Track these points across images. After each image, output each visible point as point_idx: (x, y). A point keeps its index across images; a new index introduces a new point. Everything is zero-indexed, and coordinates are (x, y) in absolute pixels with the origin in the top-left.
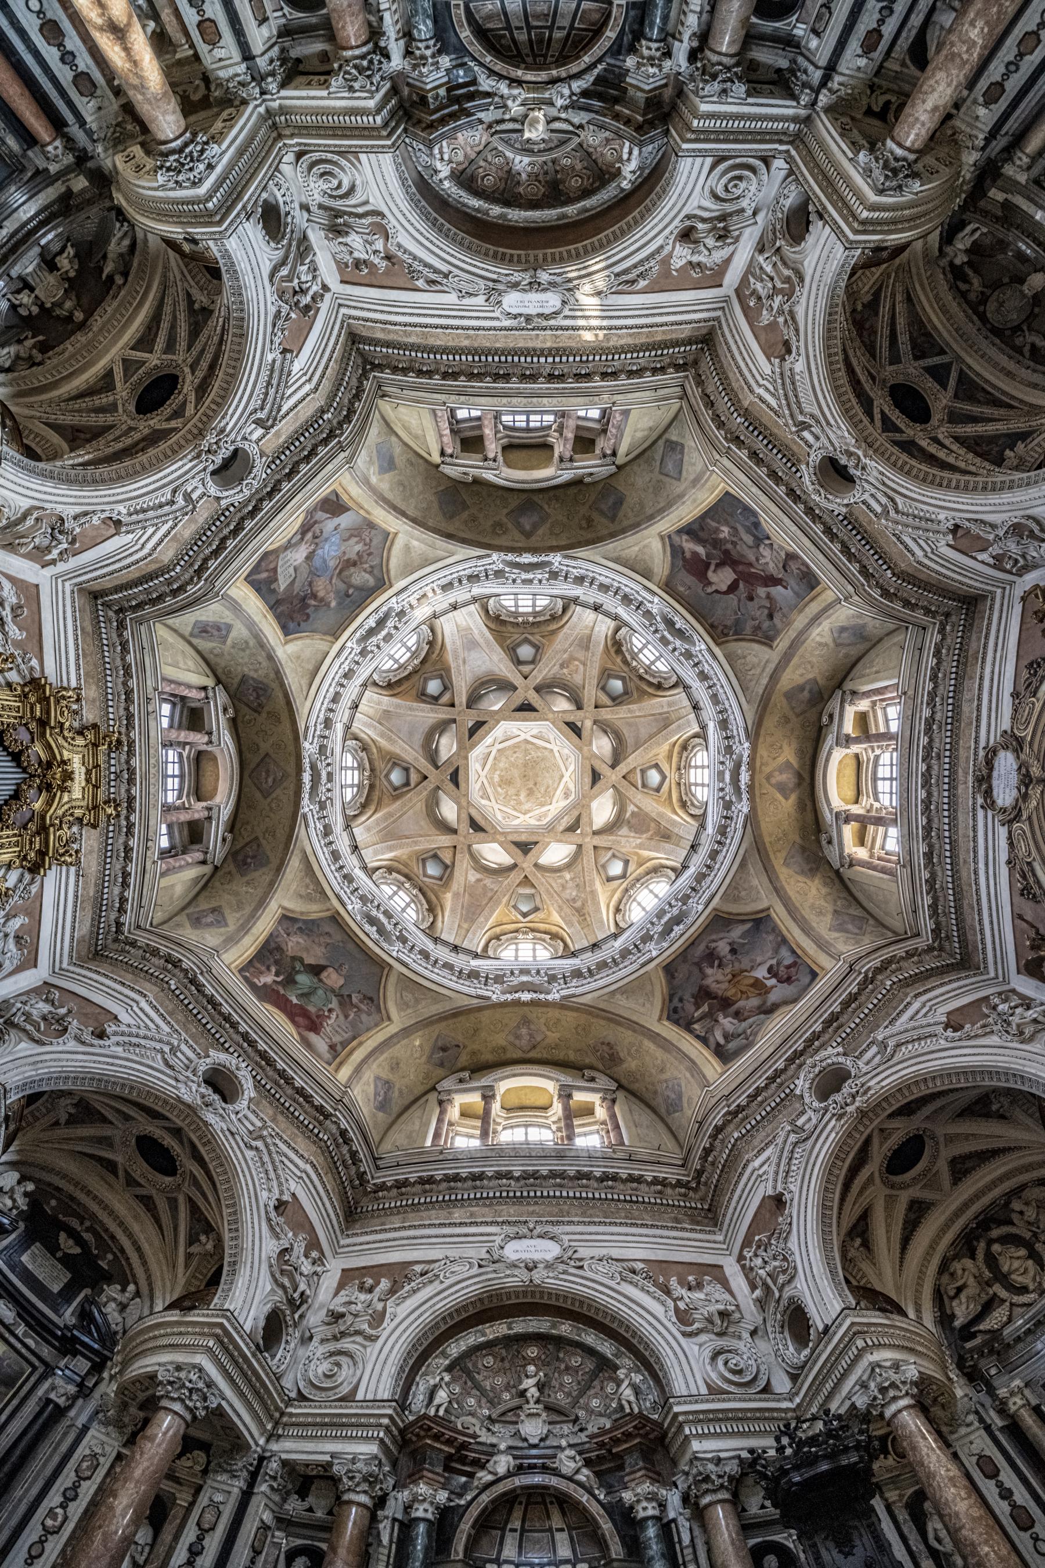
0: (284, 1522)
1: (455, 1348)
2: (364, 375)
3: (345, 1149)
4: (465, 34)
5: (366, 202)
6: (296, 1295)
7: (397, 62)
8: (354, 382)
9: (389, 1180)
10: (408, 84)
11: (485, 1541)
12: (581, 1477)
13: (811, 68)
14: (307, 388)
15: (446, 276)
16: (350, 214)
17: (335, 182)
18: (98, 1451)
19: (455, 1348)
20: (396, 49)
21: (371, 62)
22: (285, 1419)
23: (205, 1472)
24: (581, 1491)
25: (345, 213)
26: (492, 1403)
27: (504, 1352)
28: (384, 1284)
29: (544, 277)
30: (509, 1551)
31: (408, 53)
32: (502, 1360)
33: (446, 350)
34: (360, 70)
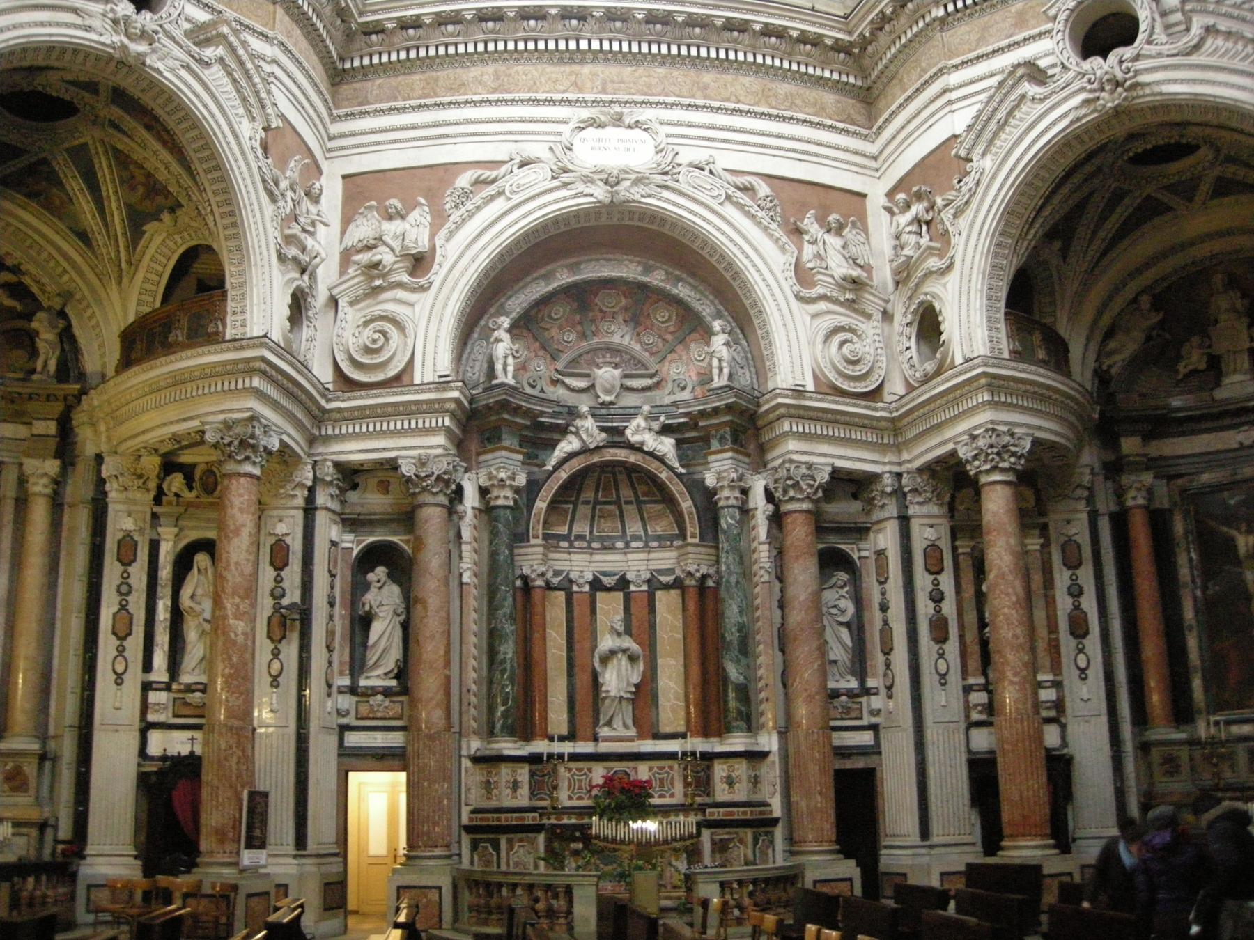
2: (865, 43)
4: (686, 504)
5: (815, 316)
7: (758, 485)
8: (883, 39)
10: (748, 455)
13: (329, 504)
14: (954, 78)
15: (728, 197)
16: (835, 301)
17: (846, 349)
20: (758, 500)
21: (785, 492)
25: (841, 304)
29: (600, 193)
31: (745, 492)
33: (737, 66)
34: (796, 485)
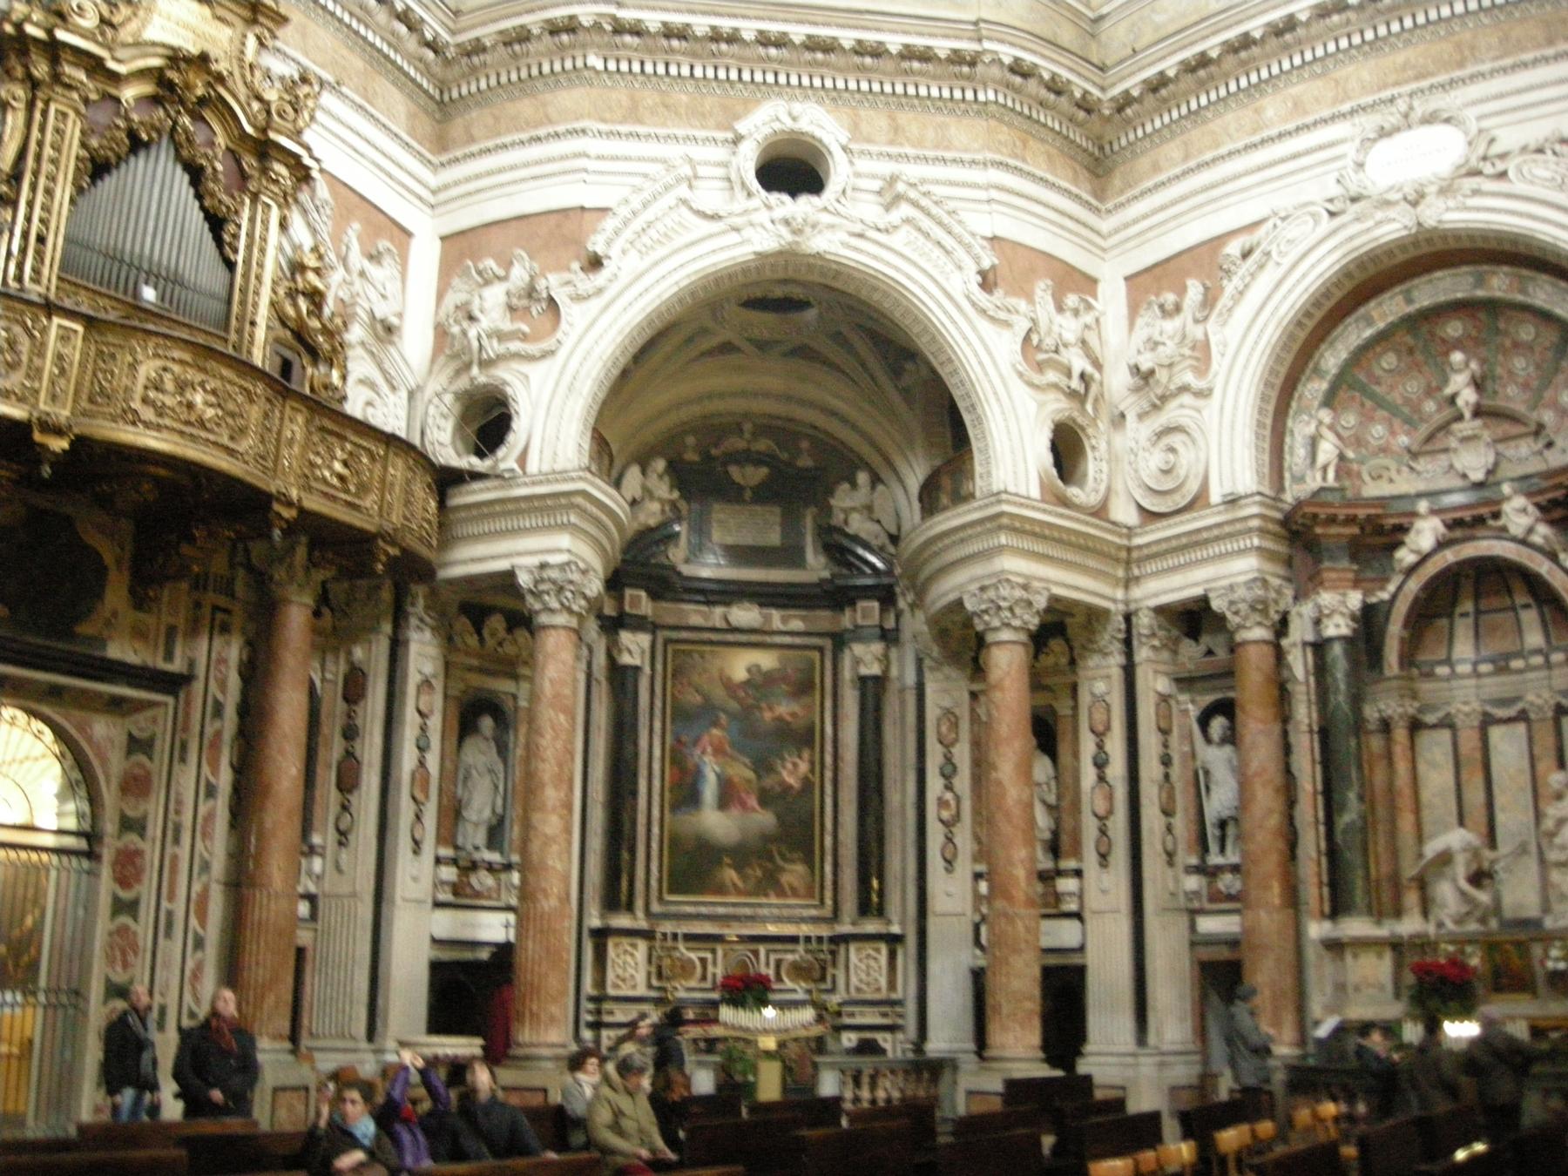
0: (1185, 682)
1: (1332, 359)
3: (1032, 86)
6: (1076, 384)
9: (1132, 83)
11: (1429, 637)
12: (1537, 539)
18: (947, 703)
19: (1332, 359)
22: (1135, 554)
23: (1073, 662)
24: (1539, 557)
26: (1410, 423)
27: (1409, 340)
28: (1194, 291)
30: (1464, 648)
32: (1411, 351)
